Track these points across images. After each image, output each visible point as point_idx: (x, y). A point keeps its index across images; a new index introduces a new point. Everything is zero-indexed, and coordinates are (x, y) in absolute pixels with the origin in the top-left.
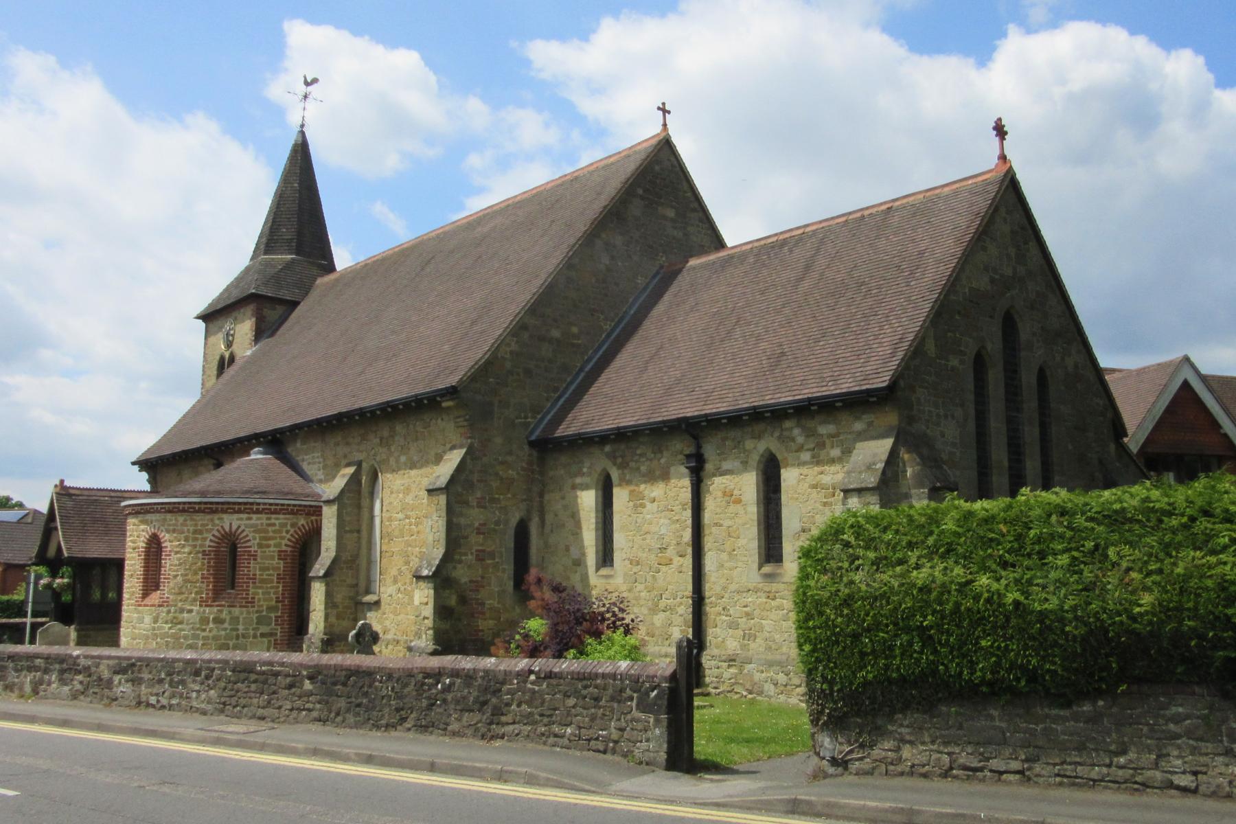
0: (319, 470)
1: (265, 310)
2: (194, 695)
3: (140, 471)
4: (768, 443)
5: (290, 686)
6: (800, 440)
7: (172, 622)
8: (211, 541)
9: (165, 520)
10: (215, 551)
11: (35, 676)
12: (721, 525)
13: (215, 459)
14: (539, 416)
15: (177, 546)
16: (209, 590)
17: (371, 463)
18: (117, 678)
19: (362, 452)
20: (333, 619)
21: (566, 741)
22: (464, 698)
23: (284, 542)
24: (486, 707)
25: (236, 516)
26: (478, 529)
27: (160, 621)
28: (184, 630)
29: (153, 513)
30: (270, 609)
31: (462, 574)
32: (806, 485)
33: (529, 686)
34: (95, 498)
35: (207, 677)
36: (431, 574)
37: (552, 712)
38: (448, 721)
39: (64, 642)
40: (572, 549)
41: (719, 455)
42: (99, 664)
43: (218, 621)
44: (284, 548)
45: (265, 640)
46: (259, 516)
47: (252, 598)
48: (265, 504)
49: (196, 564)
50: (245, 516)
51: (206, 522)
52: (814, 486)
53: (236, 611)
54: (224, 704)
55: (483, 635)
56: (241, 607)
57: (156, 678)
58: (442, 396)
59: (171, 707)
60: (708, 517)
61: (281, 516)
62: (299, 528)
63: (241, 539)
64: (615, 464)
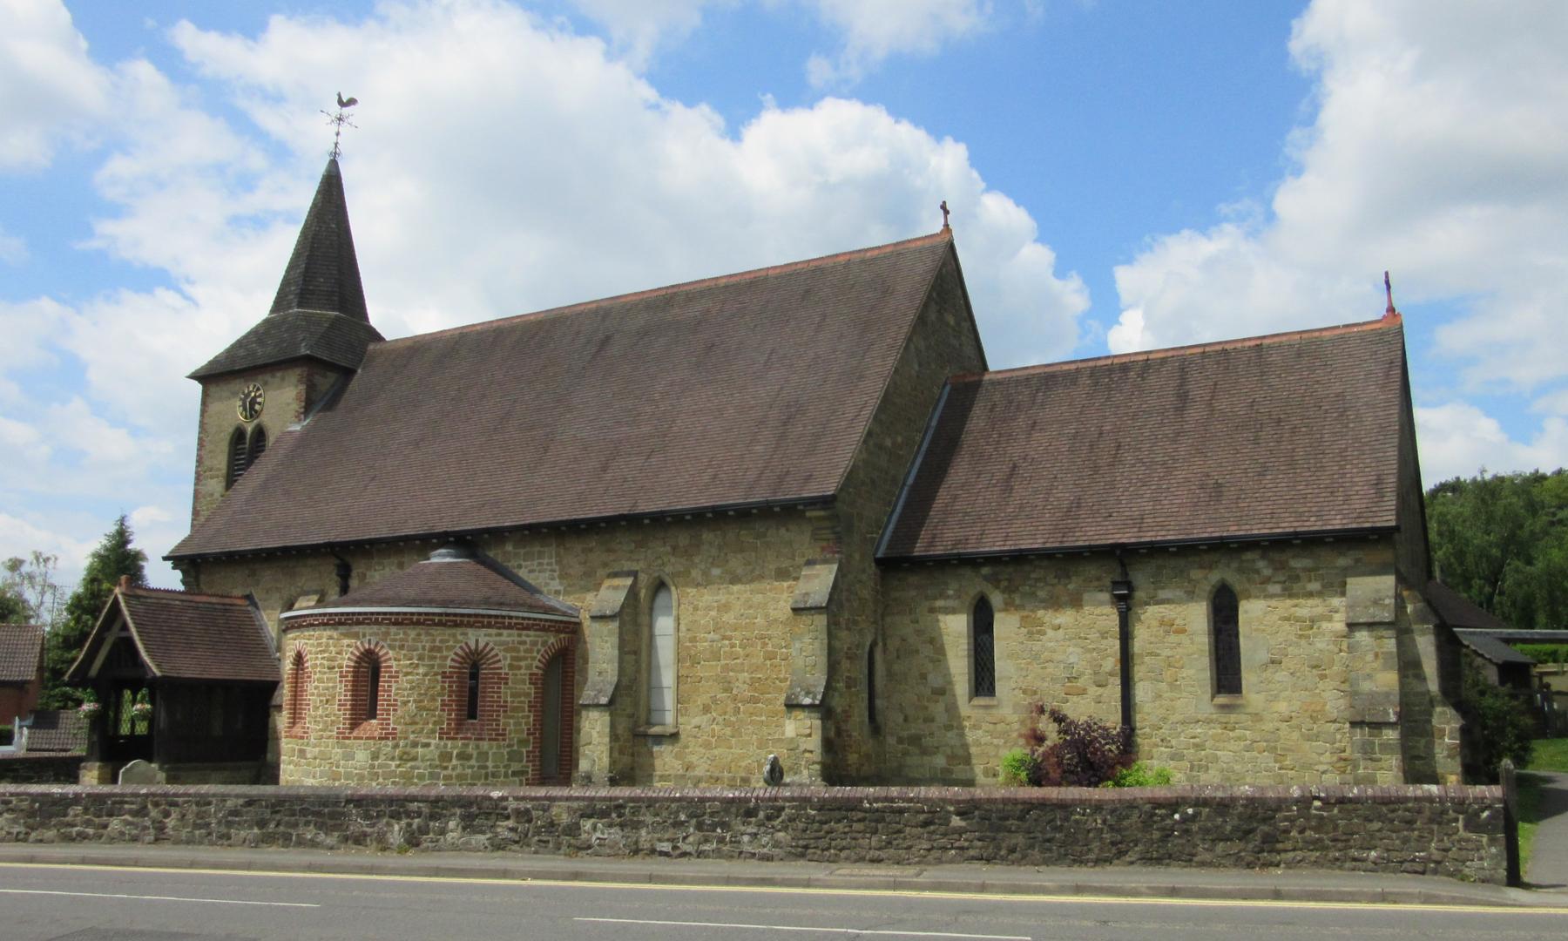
0: (553, 579)
2: (746, 838)
4: (1222, 573)
5: (925, 824)
6: (1267, 572)
7: (401, 759)
8: (453, 660)
11: (409, 825)
12: (1158, 655)
13: (342, 560)
15: (407, 666)
16: (452, 719)
17: (656, 575)
18: (587, 825)
20: (616, 754)
21: (1371, 866)
22: (1217, 827)
23: (536, 663)
24: (1251, 836)
25: (484, 631)
27: (382, 757)
28: (418, 768)
29: (368, 624)
30: (522, 742)
31: (838, 703)
33: (1314, 812)
34: (164, 601)
35: (769, 818)
36: (817, 702)
37: (1349, 837)
38: (1194, 851)
39: (150, 780)
40: (930, 677)
41: (1153, 583)
42: (549, 807)
43: (463, 756)
45: (517, 779)
46: (509, 631)
47: (503, 730)
48: (517, 618)
49: (434, 687)
50: (493, 631)
51: (446, 637)
52: (1287, 619)
53: (485, 745)
54: (806, 847)
56: (490, 740)
57: (670, 821)
58: (805, 505)
59: (700, 854)
60: (1138, 645)
61: (531, 633)
64: (997, 587)
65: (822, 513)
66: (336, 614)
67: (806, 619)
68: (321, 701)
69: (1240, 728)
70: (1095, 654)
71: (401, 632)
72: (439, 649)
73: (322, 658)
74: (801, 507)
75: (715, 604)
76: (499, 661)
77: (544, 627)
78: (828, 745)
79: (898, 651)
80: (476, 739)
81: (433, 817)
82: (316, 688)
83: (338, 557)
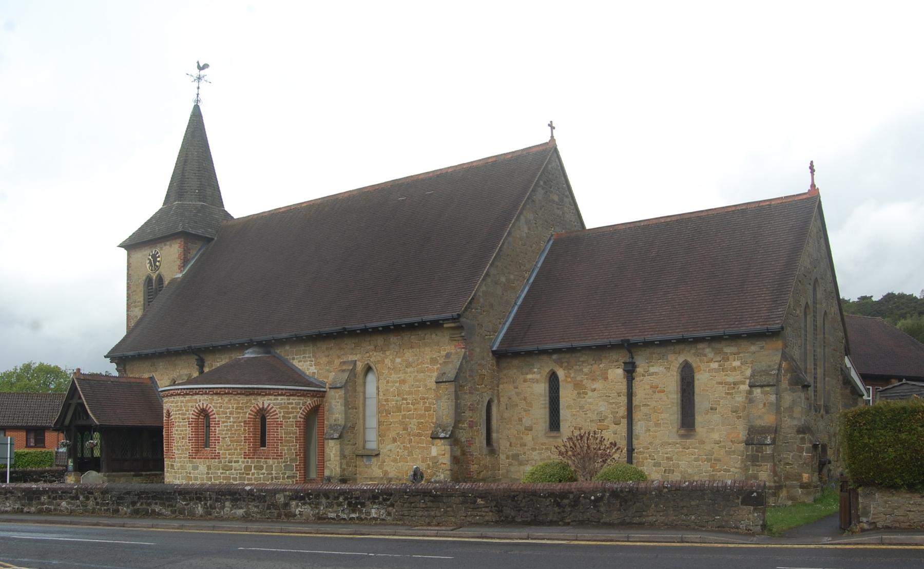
3: (111, 362)
10: (254, 421)
11: (206, 504)
13: (199, 356)
14: (496, 334)
16: (250, 447)
17: (366, 362)
18: (294, 503)
19: (356, 354)
23: (299, 415)
25: (266, 398)
26: (470, 407)
29: (202, 394)
30: (292, 460)
31: (463, 436)
40: (524, 420)
44: (299, 419)
50: (273, 397)
53: (270, 462)
55: (473, 475)
56: (273, 459)
62: (307, 406)
63: (271, 413)
65: (452, 325)
66: (184, 389)
67: (443, 386)
68: (180, 438)
69: (692, 448)
70: (614, 406)
71: (220, 398)
72: (242, 408)
73: (179, 414)
74: (441, 322)
75: (398, 380)
76: (277, 414)
77: (303, 394)
78: (455, 460)
79: (506, 405)
80: (265, 458)
81: (217, 500)
82: (177, 430)
83: (196, 354)
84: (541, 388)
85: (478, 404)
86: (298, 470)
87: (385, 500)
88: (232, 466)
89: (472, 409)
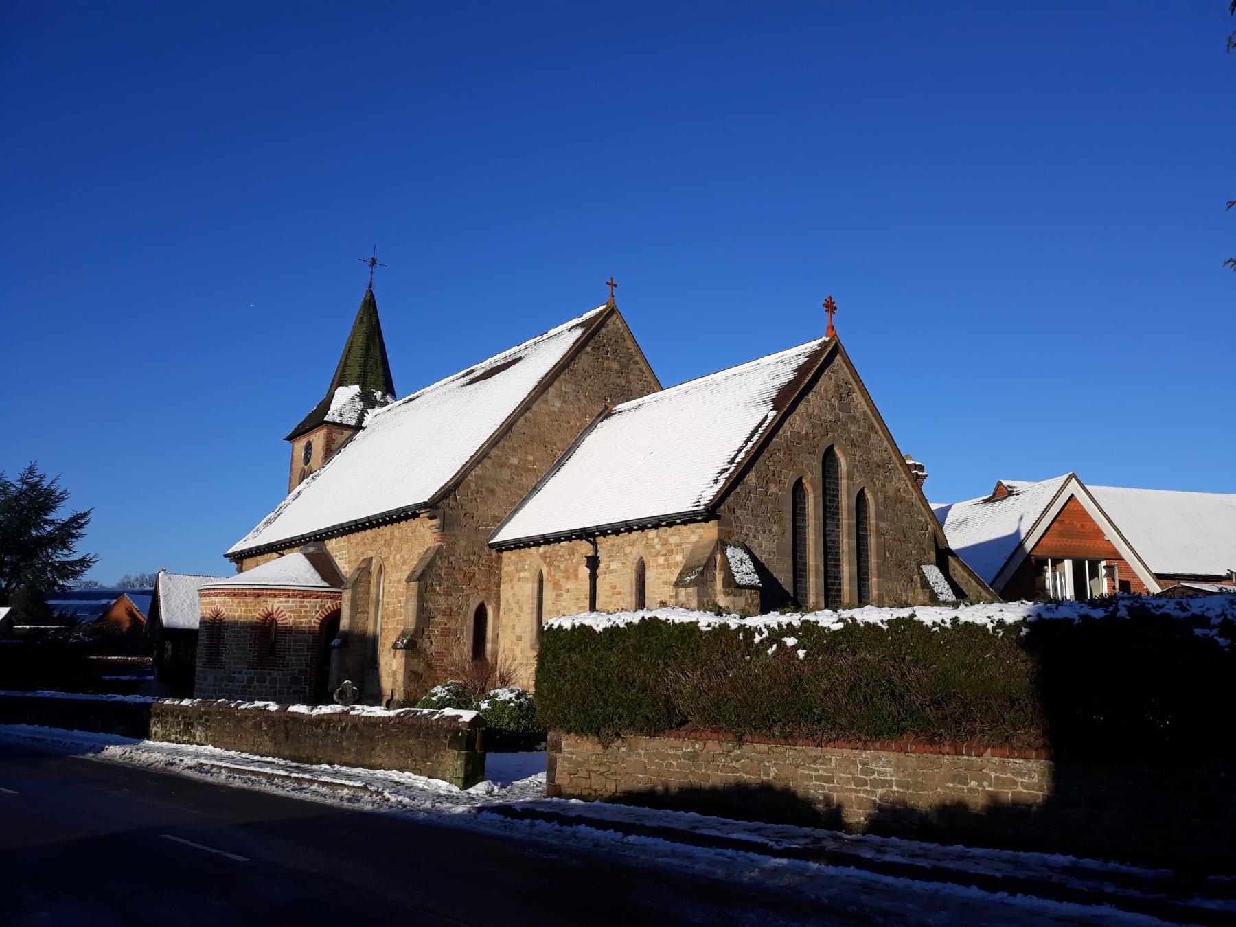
1: (334, 434)
6: (658, 547)
8: (257, 618)
9: (225, 602)
25: (276, 600)
30: (300, 672)
32: (661, 581)
43: (262, 680)
44: (313, 625)
45: (296, 696)
47: (288, 663)
53: (275, 673)
61: (312, 600)
76: (286, 619)
84: (530, 588)
85: (461, 607)
86: (307, 685)
87: (207, 720)
88: (235, 677)
89: (449, 613)
